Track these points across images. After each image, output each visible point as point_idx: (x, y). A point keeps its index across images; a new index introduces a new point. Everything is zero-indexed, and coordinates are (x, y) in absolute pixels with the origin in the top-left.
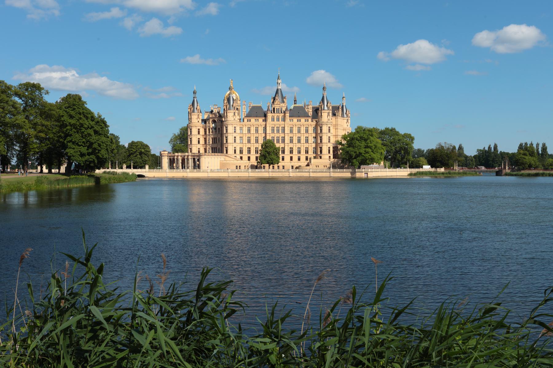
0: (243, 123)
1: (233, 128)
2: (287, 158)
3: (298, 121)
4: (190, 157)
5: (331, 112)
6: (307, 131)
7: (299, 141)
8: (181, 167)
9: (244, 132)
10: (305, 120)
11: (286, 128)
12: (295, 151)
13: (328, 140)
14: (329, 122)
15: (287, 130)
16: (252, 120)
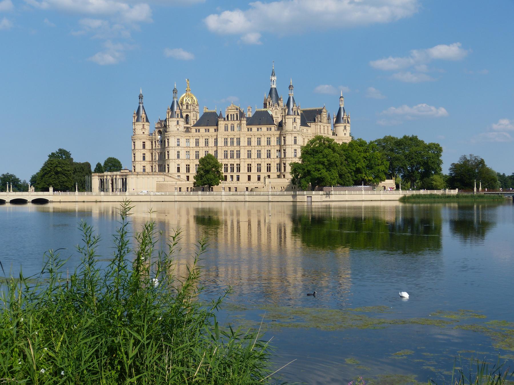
0: (190, 134)
1: (176, 140)
2: (244, 177)
3: (258, 130)
4: (118, 177)
5: (299, 117)
6: (269, 143)
7: (259, 156)
8: (111, 190)
9: (191, 146)
10: (206, 130)
11: (242, 140)
12: (254, 169)
13: (293, 154)
14: (295, 130)
15: (244, 142)
16: (210, 129)
